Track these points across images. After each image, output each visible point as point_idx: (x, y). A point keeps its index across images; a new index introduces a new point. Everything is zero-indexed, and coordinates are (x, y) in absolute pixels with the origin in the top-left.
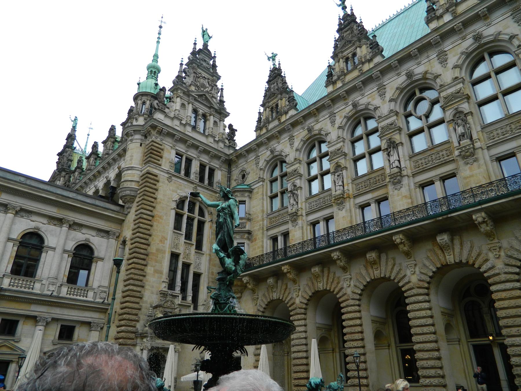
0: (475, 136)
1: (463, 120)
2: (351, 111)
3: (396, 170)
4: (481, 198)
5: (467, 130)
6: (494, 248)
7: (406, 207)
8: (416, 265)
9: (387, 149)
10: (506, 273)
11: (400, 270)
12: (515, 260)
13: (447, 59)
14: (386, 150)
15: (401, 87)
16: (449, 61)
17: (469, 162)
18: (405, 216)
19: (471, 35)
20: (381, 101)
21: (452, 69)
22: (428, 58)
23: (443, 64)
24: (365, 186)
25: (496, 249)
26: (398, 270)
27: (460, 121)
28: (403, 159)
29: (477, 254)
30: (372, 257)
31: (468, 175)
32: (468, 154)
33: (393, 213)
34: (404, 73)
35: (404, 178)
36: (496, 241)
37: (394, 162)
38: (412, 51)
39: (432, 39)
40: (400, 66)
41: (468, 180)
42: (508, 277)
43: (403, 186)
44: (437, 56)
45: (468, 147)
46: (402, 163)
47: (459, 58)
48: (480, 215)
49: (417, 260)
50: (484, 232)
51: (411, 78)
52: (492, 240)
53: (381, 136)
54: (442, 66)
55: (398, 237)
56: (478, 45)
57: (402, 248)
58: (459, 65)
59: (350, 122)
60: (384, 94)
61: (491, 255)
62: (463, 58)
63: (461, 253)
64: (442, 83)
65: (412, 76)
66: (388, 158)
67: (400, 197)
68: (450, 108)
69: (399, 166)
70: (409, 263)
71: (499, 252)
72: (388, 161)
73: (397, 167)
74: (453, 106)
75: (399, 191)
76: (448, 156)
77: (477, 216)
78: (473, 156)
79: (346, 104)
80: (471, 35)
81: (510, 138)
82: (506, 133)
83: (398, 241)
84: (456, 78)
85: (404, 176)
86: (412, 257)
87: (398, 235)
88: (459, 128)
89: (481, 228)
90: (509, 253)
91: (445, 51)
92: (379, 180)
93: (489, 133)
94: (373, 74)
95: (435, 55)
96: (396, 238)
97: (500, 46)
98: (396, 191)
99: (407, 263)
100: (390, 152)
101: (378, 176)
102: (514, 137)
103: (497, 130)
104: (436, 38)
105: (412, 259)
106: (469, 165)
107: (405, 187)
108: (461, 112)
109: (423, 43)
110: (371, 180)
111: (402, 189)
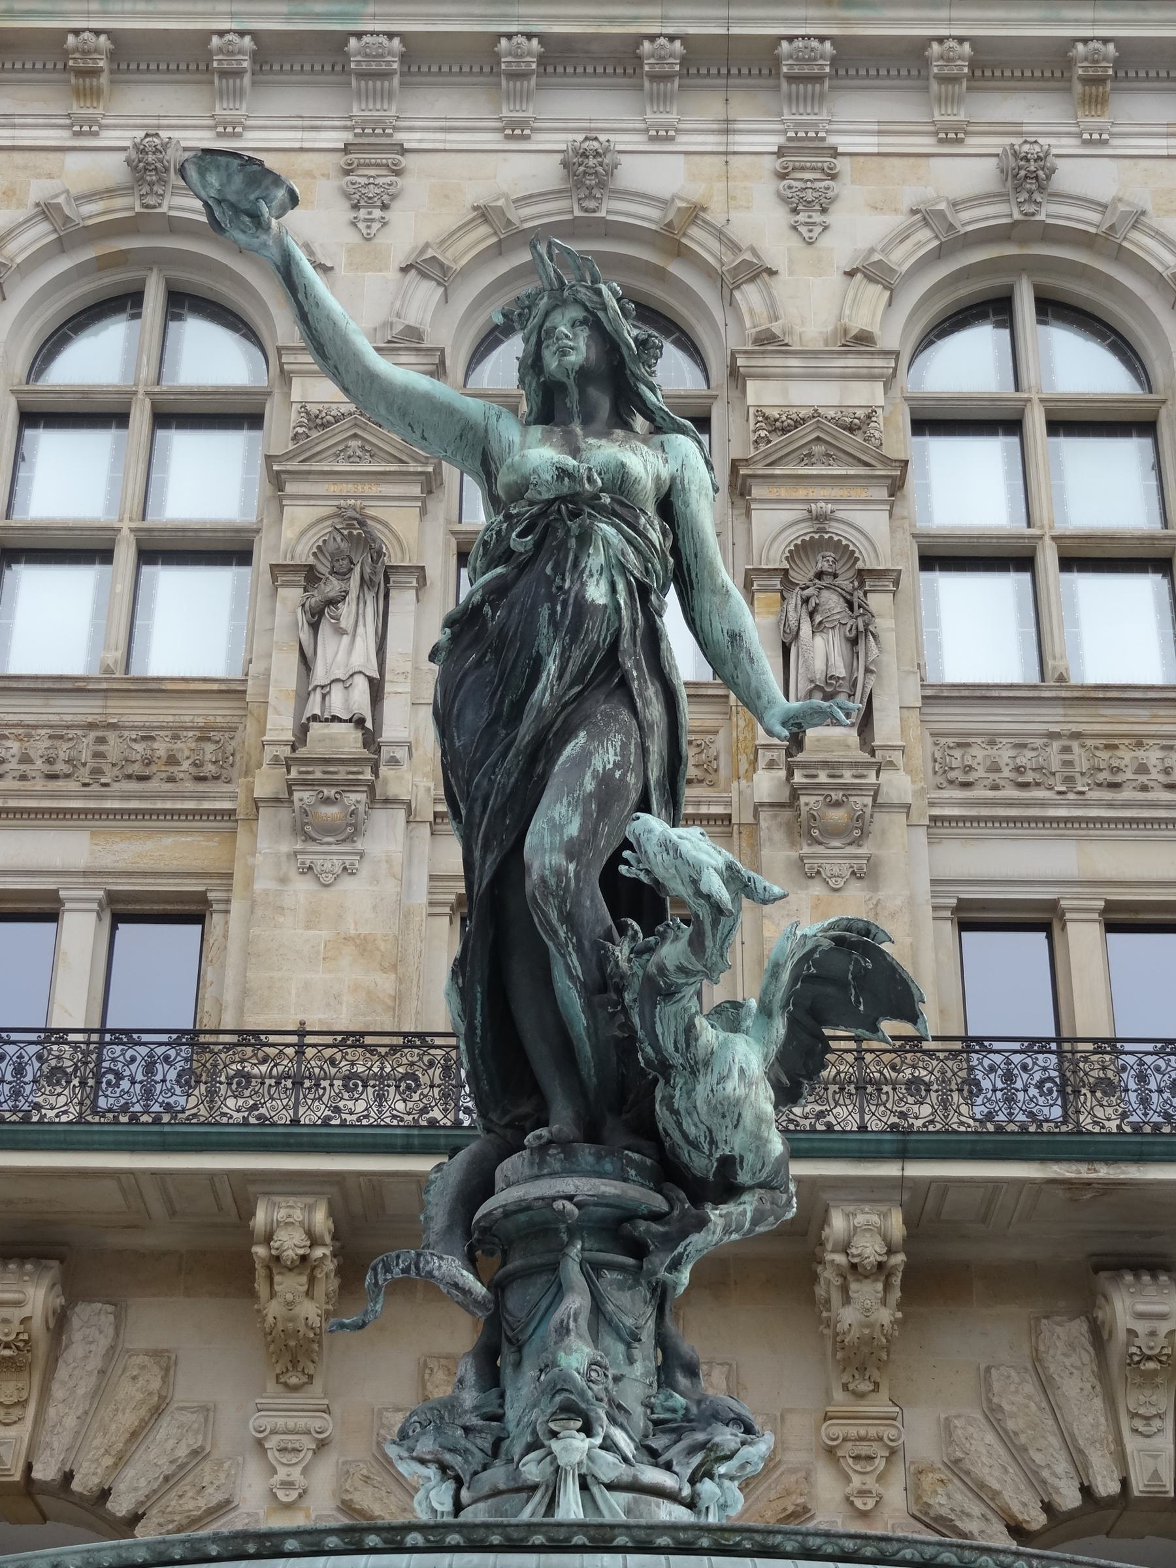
0: (886, 728)
1: (850, 605)
2: (110, 193)
3: (348, 740)
4: (903, 1115)
5: (860, 675)
6: (864, 1449)
7: (344, 1022)
8: (322, 1445)
9: (311, 576)
11: (195, 1453)
13: (832, 200)
14: (300, 578)
15: (515, 215)
16: (835, 217)
17: (828, 868)
18: (381, 1078)
19: (996, 144)
20: (352, 237)
21: (851, 274)
22: (727, 132)
23: (802, 217)
24: (50, 761)
25: (870, 1458)
26: (182, 1452)
27: (832, 602)
28: (406, 687)
30: (16, 1314)
32: (837, 816)
33: (302, 1033)
34: (561, 141)
35: (380, 816)
36: (880, 1405)
37: (345, 683)
38: (652, 38)
39: (791, 39)
40: (539, 87)
43: (365, 870)
44: (780, 153)
45: (848, 777)
46: (390, 706)
47: (903, 236)
48: (875, 1218)
49: (335, 1408)
50: (855, 1334)
51: (591, 196)
52: (861, 1396)
53: (293, 466)
54: (795, 228)
55: (298, 1215)
56: (1017, 216)
57: (290, 1305)
58: (892, 270)
59: (64, 264)
60: (385, 207)
62: (918, 245)
64: (776, 328)
65: (602, 185)
66: (305, 635)
67: (324, 934)
68: (783, 493)
69: (369, 724)
70: (281, 1422)
71: (880, 1478)
72: (296, 655)
73: (359, 722)
74: (801, 493)
75: (326, 894)
77: (860, 1219)
78: (857, 842)
79: (84, 128)
80: (996, 144)
81: (1058, 820)
82: (1038, 777)
83: (291, 1242)
84: (864, 339)
85: (387, 801)
86: (317, 1386)
87: (300, 1201)
88: (819, 640)
89: (847, 1300)
90: (940, 1503)
91: (834, 152)
92: (172, 760)
93: (951, 741)
94: (359, 35)
95: (772, 142)
96: (280, 1215)
97: (1110, 284)
98: (302, 887)
99: (267, 1421)
100: (332, 602)
101: (176, 732)
103: (992, 743)
104: (815, 44)
105: (314, 1395)
106: (817, 889)
107: (375, 880)
108: (846, 553)
109: (735, 30)
110: (111, 736)
111: (348, 884)
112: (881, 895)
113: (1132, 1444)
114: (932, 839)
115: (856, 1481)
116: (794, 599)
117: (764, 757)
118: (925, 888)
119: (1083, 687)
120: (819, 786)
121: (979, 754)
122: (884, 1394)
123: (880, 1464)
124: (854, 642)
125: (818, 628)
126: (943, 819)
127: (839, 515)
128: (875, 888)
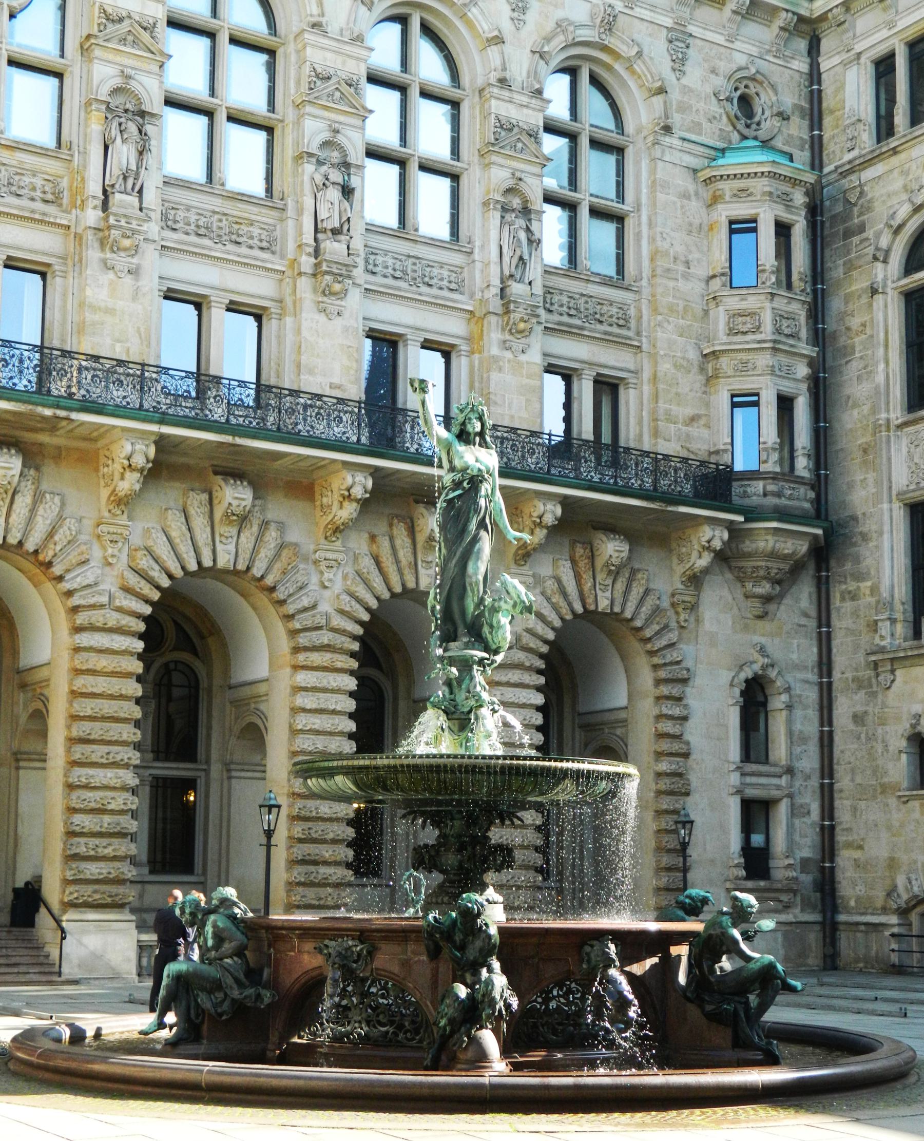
1: (140, 132)
4: (159, 403)
6: (114, 537)
10: (119, 610)
12: (149, 585)
27: (132, 128)
29: (69, 538)
31: (103, 305)
32: (126, 243)
41: (97, 317)
42: (123, 622)
61: (97, 553)
63: (30, 520)
68: (110, 57)
74: (118, 59)
76: (46, 201)
78: (132, 256)
88: (125, 148)
102: (224, 259)
106: (111, 275)
112: (140, 284)
113: (219, 547)
114: (161, 255)
115: (110, 551)
116: (115, 124)
117: (91, 203)
118: (156, 280)
119: (232, 192)
120: (121, 227)
121: (181, 214)
122: (125, 516)
123: (120, 544)
124: (141, 153)
125: (124, 141)
126: (168, 247)
127: (137, 77)
128: (137, 280)
